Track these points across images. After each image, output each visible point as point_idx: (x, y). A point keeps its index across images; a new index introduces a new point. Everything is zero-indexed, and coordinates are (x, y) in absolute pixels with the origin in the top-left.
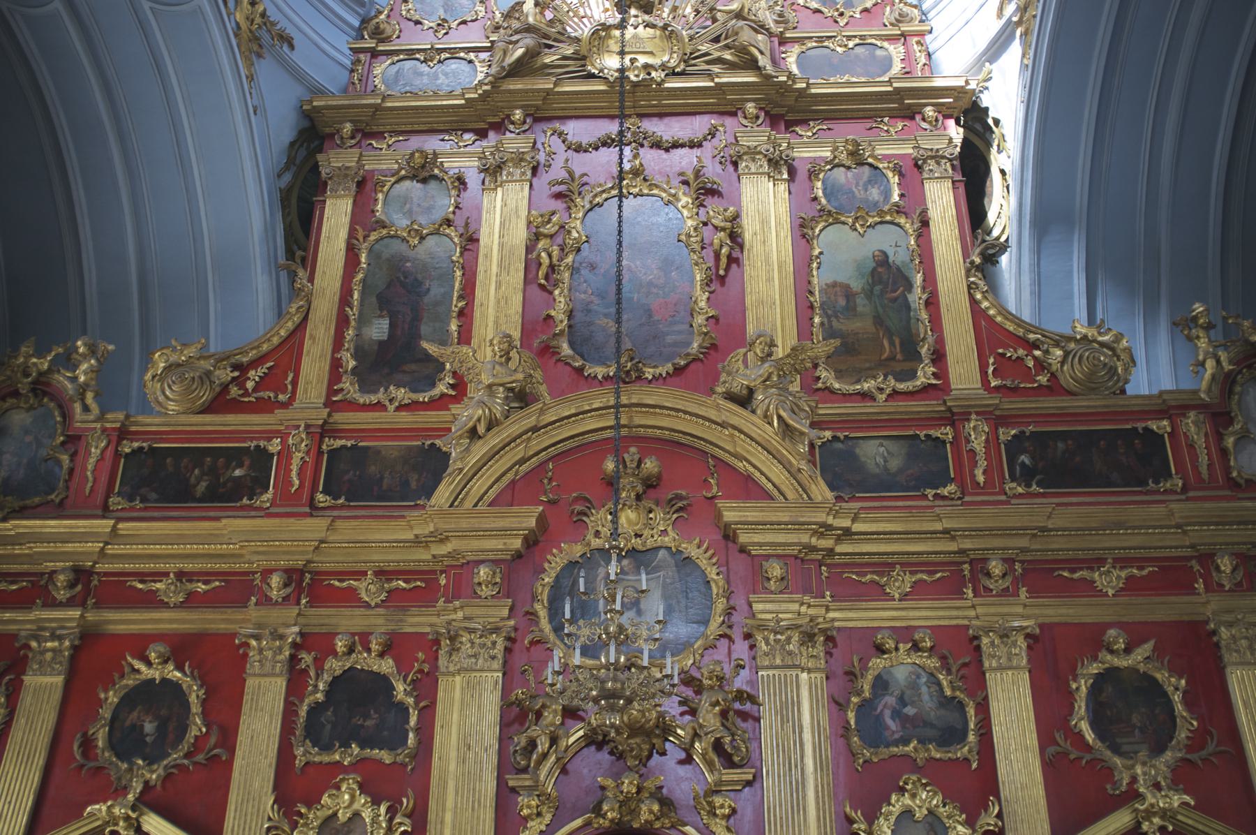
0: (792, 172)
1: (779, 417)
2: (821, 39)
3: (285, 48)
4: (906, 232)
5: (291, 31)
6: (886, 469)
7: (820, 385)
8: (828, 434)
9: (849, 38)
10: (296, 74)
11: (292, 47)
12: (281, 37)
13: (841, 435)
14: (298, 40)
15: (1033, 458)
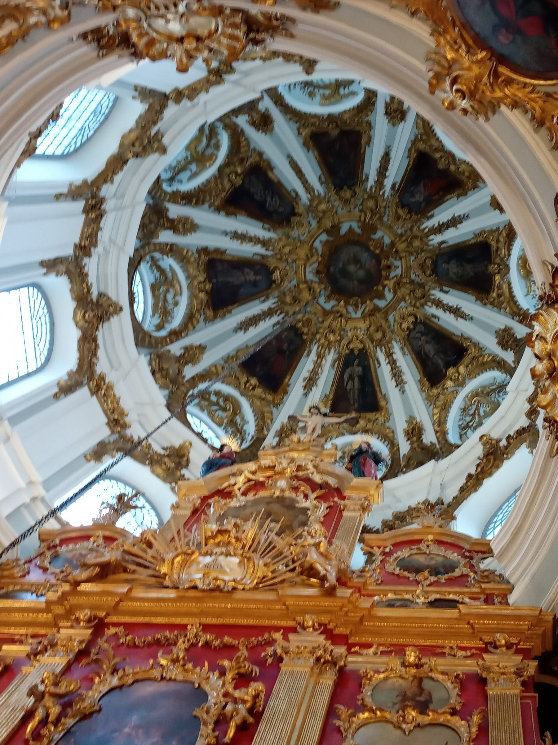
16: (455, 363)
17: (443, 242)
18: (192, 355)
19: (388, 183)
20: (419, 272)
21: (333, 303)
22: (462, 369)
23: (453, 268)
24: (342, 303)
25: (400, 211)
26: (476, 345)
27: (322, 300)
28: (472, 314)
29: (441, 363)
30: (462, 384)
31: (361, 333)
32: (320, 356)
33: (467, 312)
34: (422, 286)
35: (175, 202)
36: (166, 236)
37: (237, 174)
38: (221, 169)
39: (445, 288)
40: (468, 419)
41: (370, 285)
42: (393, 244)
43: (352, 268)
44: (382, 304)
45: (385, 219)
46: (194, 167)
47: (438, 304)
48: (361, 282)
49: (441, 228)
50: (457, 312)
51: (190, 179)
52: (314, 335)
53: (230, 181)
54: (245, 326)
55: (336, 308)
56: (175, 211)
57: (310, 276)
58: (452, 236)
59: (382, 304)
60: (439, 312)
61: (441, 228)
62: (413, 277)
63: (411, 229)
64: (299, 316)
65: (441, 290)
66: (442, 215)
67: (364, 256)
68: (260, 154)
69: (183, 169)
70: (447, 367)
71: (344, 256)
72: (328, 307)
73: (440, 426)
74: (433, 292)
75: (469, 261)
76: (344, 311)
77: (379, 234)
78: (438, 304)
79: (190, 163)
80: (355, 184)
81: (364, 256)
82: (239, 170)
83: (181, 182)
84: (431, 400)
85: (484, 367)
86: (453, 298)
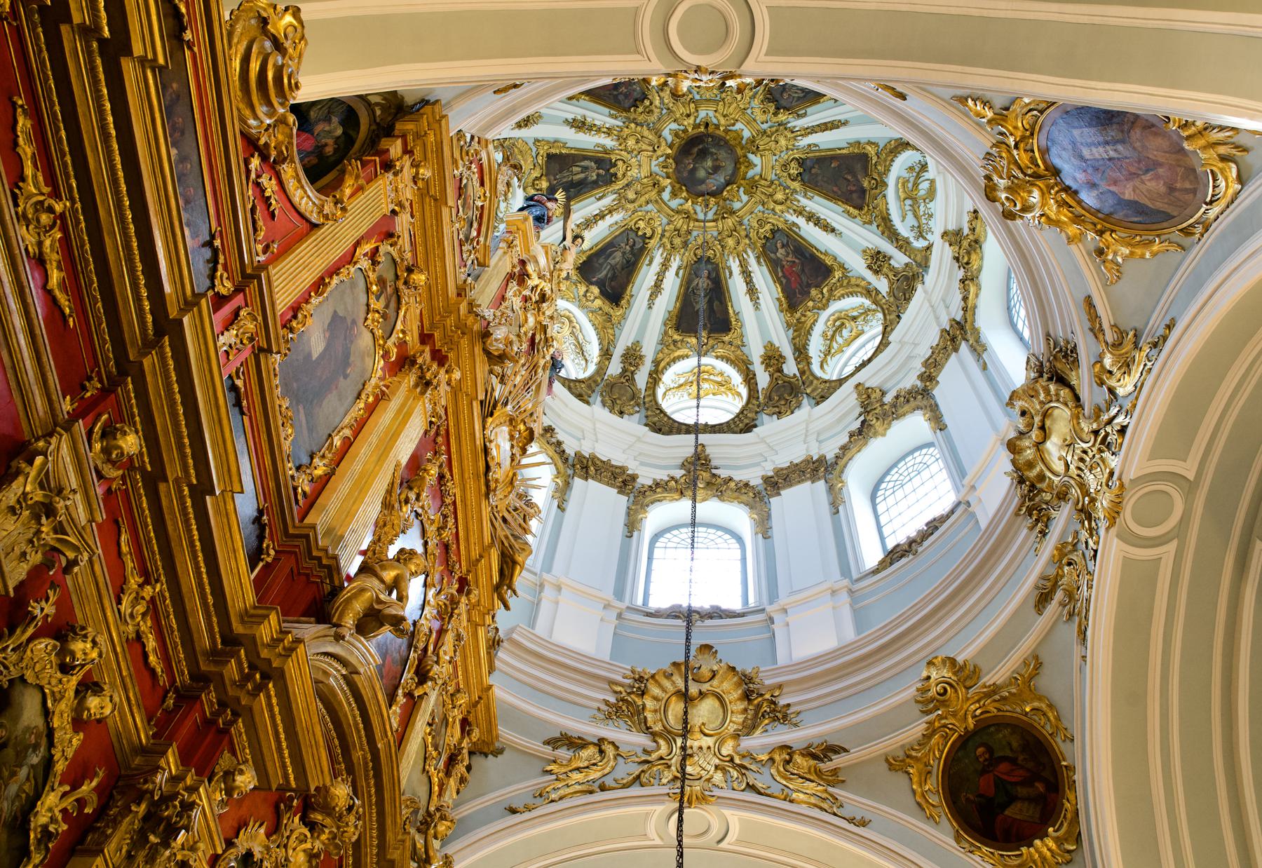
16: (604, 293)
17: (731, 273)
19: (801, 221)
20: (700, 241)
21: (670, 139)
22: (598, 303)
23: (703, 283)
24: (669, 151)
25: (768, 227)
26: (624, 317)
27: (674, 126)
28: (655, 307)
30: (582, 307)
31: (634, 172)
32: (609, 132)
33: (657, 301)
34: (685, 244)
39: (681, 272)
41: (688, 183)
42: (733, 212)
43: (709, 163)
44: (666, 195)
45: (760, 208)
47: (665, 266)
49: (747, 274)
50: (657, 287)
52: (634, 121)
55: (663, 144)
57: (702, 114)
58: (737, 285)
59: (666, 195)
60: (656, 267)
61: (747, 274)
62: (695, 233)
63: (747, 236)
64: (657, 102)
65: (679, 268)
66: (761, 276)
67: (721, 178)
70: (600, 284)
71: (722, 154)
72: (666, 133)
74: (678, 258)
75: (710, 302)
76: (659, 153)
77: (745, 198)
78: (665, 266)
80: (803, 182)
81: (721, 178)
85: (601, 330)
86: (672, 283)
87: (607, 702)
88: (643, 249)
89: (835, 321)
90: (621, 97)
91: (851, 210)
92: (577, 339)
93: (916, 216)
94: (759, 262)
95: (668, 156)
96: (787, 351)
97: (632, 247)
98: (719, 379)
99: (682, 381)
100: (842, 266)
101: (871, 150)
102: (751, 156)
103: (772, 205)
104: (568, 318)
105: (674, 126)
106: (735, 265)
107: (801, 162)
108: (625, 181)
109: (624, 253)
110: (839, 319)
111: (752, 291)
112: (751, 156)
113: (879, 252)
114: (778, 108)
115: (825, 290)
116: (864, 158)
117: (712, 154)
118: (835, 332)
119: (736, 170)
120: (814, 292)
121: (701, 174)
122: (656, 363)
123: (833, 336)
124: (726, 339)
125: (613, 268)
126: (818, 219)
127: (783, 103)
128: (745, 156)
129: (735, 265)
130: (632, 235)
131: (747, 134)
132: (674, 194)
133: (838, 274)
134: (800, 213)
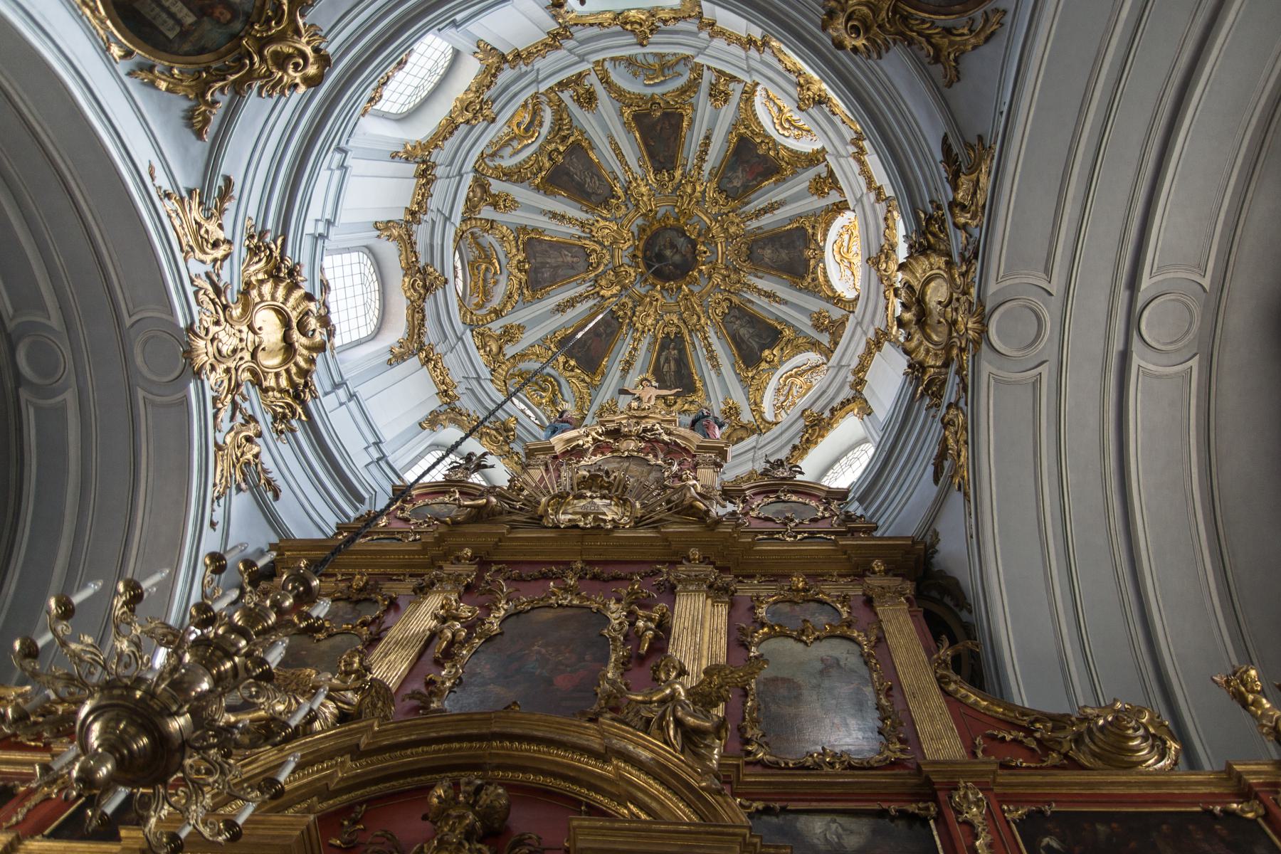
0: (732, 606)
1: (679, 723)
2: (773, 533)
3: (270, 494)
4: (859, 644)
5: (280, 483)
6: (840, 844)
7: (751, 758)
8: (759, 805)
9: (800, 533)
10: (273, 520)
11: (276, 497)
12: (269, 484)
13: (777, 805)
14: (285, 493)
15: (1062, 840)
16: (771, 347)
17: (759, 228)
18: (509, 335)
19: (707, 167)
21: (648, 287)
29: (756, 346)
30: (775, 368)
35: (498, 178)
36: (486, 212)
37: (560, 153)
38: (541, 148)
40: (782, 398)
43: (668, 253)
46: (515, 143)
48: (676, 266)
51: (511, 156)
53: (551, 159)
54: (560, 309)
56: (496, 186)
59: (696, 289)
60: (754, 298)
63: (727, 215)
66: (759, 202)
68: (583, 132)
69: (507, 144)
70: (762, 350)
72: (643, 291)
73: (756, 407)
79: (511, 139)
80: (674, 168)
81: (681, 241)
82: (561, 149)
83: (502, 157)
84: (745, 383)
85: (798, 350)
87: (929, 408)
88: (738, 308)
89: (784, 128)
90: (609, 331)
91: (685, 124)
92: (805, 371)
93: (677, 63)
94: (748, 203)
95: (663, 288)
96: (812, 173)
97: (737, 318)
98: (846, 237)
99: (848, 273)
100: (735, 126)
101: (627, 111)
102: (659, 215)
103: (697, 194)
104: (787, 378)
105: (637, 287)
106: (754, 224)
107: (657, 171)
108: (682, 325)
109: (741, 326)
110: (781, 124)
111: (772, 208)
112: (659, 215)
113: (710, 95)
114: (613, 197)
115: (758, 140)
116: (637, 117)
117: (660, 250)
118: (795, 127)
119: (672, 228)
120: (760, 152)
121: (677, 258)
122: (828, 299)
123: (799, 128)
124: (810, 231)
125: (752, 336)
126: (701, 152)
127: (607, 192)
128: (659, 221)
129: (754, 224)
130: (728, 318)
131: (640, 221)
132: (695, 281)
133: (742, 130)
134: (700, 168)
